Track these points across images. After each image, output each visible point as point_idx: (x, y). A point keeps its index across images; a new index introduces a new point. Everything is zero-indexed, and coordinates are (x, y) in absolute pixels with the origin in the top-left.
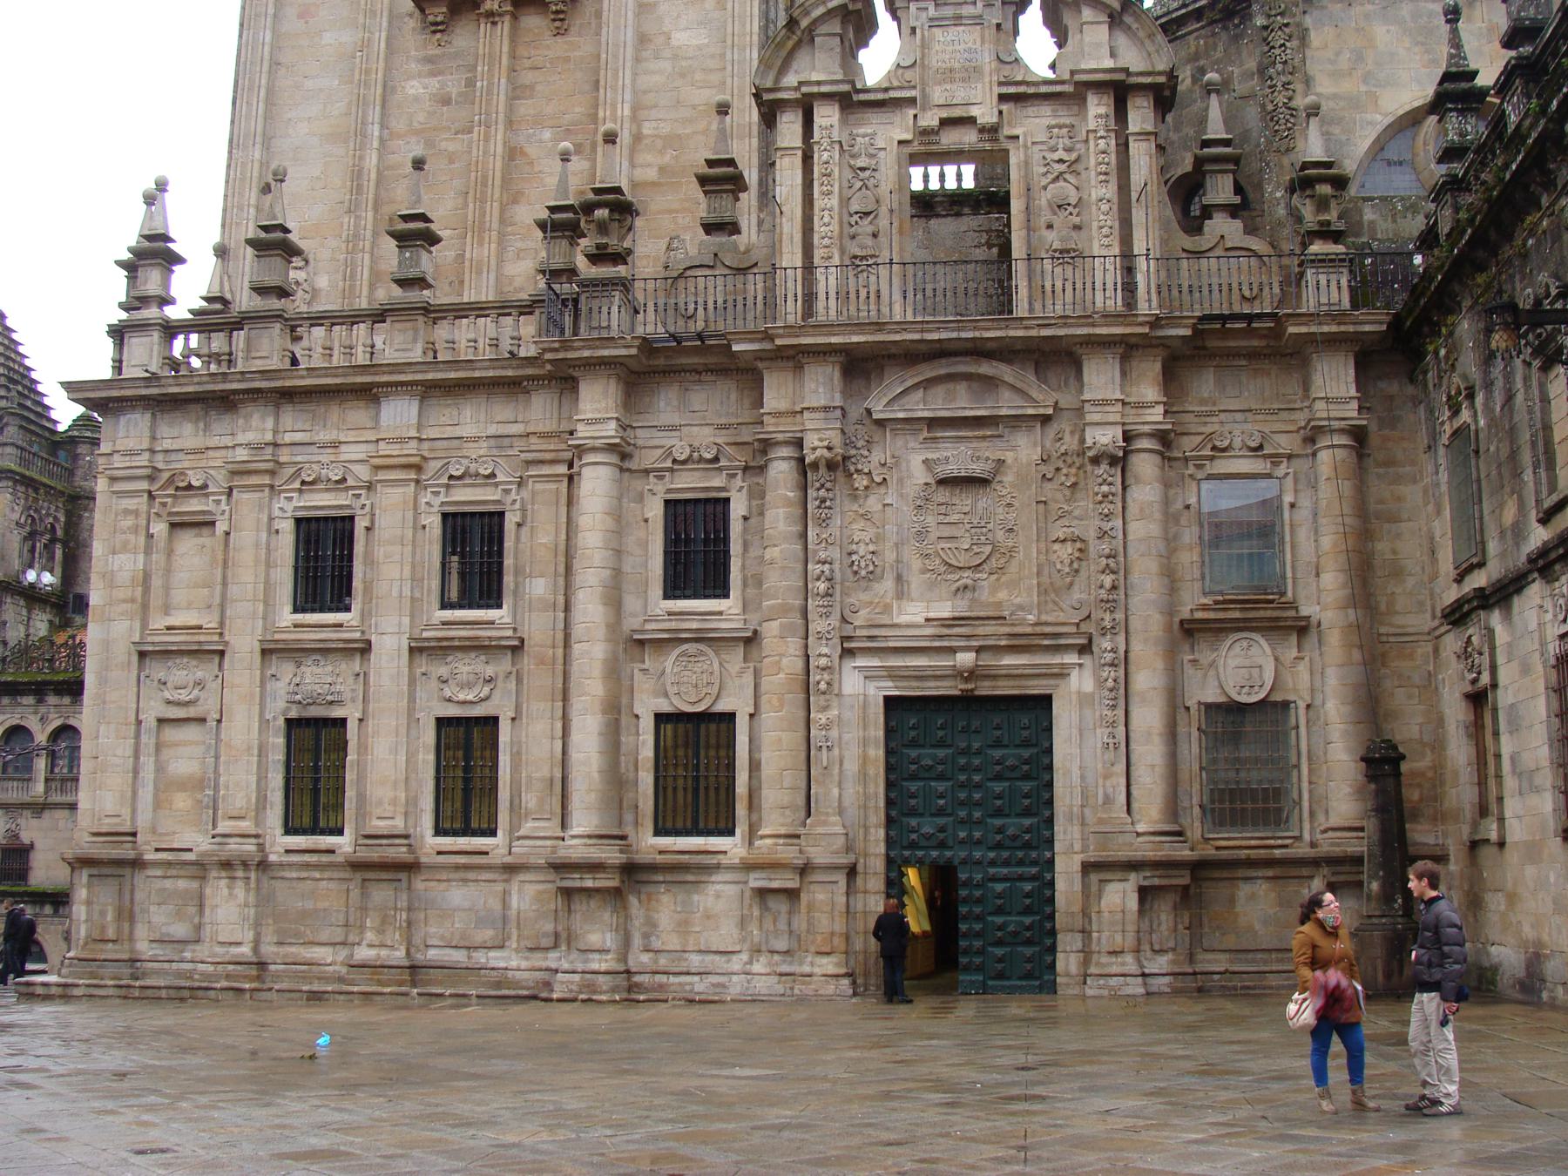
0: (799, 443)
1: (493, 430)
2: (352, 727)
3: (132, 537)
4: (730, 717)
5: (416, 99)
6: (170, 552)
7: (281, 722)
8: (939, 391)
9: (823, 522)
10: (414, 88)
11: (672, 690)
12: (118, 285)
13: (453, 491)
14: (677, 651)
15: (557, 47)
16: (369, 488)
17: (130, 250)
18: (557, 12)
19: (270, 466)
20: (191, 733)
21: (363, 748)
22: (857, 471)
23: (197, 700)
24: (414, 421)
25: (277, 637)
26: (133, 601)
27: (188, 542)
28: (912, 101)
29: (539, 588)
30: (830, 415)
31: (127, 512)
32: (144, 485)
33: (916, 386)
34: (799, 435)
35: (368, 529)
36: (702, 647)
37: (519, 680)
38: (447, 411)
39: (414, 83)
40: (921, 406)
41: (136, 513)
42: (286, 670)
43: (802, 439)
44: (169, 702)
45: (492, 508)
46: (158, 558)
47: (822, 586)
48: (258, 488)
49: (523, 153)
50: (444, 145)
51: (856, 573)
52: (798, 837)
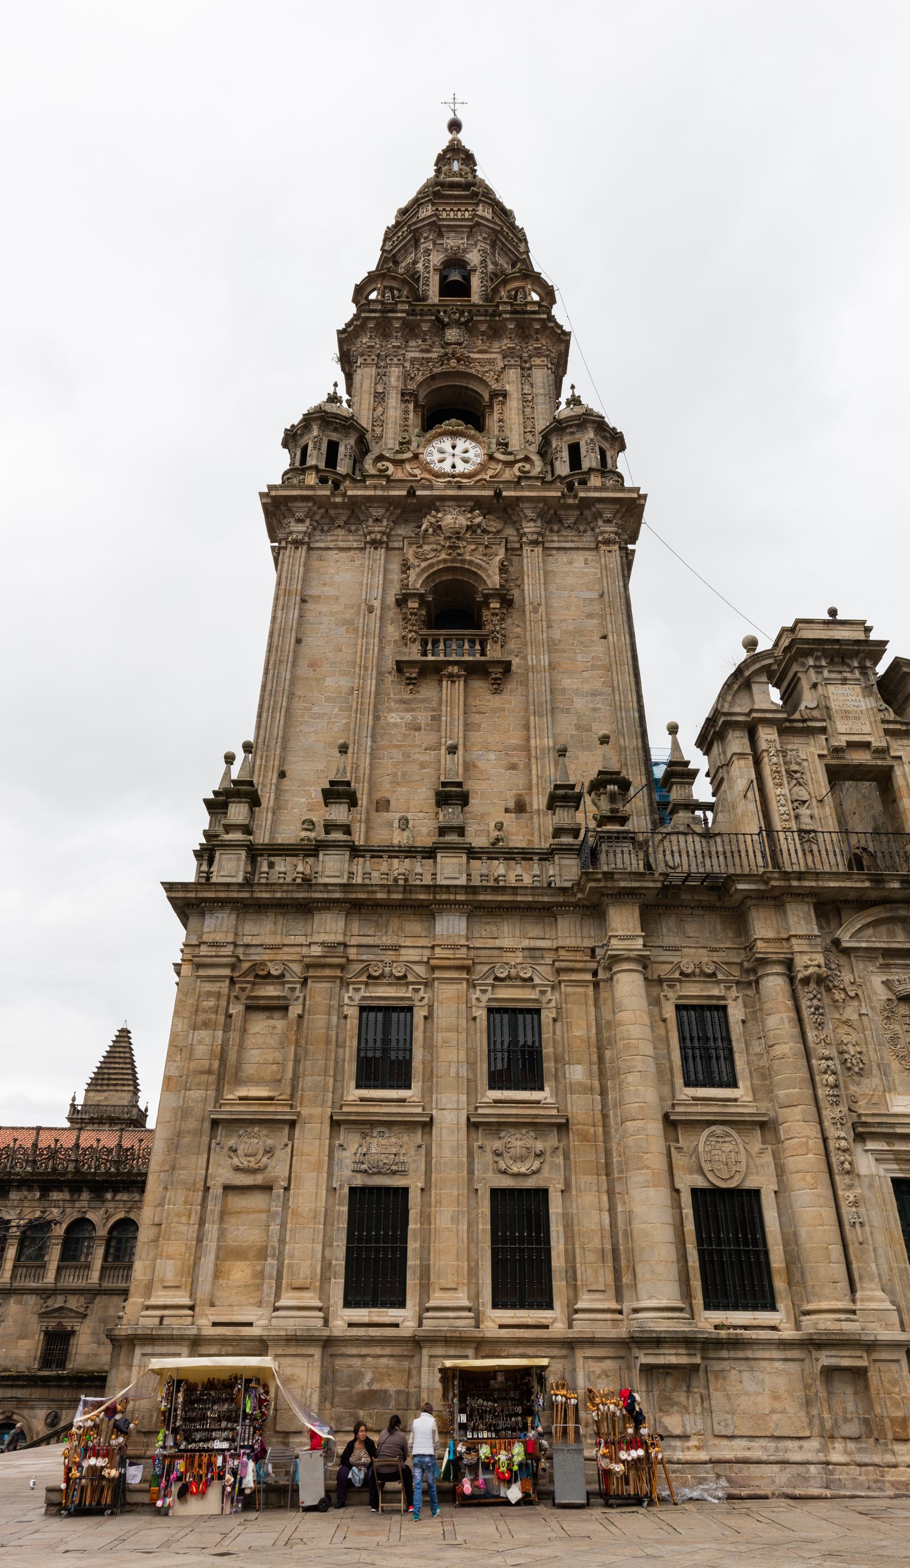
0: (789, 964)
1: (526, 943)
2: (414, 1199)
3: (213, 1016)
4: (756, 1193)
5: (395, 725)
6: (244, 1031)
7: (346, 1191)
8: (883, 929)
9: (820, 1025)
10: (393, 718)
11: (706, 1167)
12: (204, 820)
13: (497, 990)
14: (707, 1132)
15: (495, 701)
16: (426, 985)
17: (215, 793)
18: (496, 679)
19: (343, 961)
20: (257, 1201)
21: (426, 1218)
22: (835, 987)
23: (266, 1167)
24: (464, 933)
25: (345, 1109)
26: (209, 1072)
27: (260, 1025)
28: (823, 730)
29: (577, 1073)
30: (813, 942)
31: (209, 994)
32: (227, 972)
33: (867, 925)
34: (789, 956)
35: (426, 1018)
36: (728, 1129)
37: (566, 1157)
38: (488, 927)
39: (394, 715)
40: (879, 940)
41: (218, 995)
42: (352, 1143)
43: (792, 960)
44: (237, 1169)
45: (530, 1005)
46: (234, 1036)
47: (831, 1079)
48: (331, 979)
49: (475, 766)
50: (416, 756)
51: (849, 1069)
52: (854, 1312)
